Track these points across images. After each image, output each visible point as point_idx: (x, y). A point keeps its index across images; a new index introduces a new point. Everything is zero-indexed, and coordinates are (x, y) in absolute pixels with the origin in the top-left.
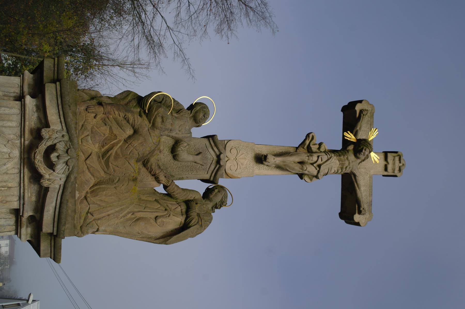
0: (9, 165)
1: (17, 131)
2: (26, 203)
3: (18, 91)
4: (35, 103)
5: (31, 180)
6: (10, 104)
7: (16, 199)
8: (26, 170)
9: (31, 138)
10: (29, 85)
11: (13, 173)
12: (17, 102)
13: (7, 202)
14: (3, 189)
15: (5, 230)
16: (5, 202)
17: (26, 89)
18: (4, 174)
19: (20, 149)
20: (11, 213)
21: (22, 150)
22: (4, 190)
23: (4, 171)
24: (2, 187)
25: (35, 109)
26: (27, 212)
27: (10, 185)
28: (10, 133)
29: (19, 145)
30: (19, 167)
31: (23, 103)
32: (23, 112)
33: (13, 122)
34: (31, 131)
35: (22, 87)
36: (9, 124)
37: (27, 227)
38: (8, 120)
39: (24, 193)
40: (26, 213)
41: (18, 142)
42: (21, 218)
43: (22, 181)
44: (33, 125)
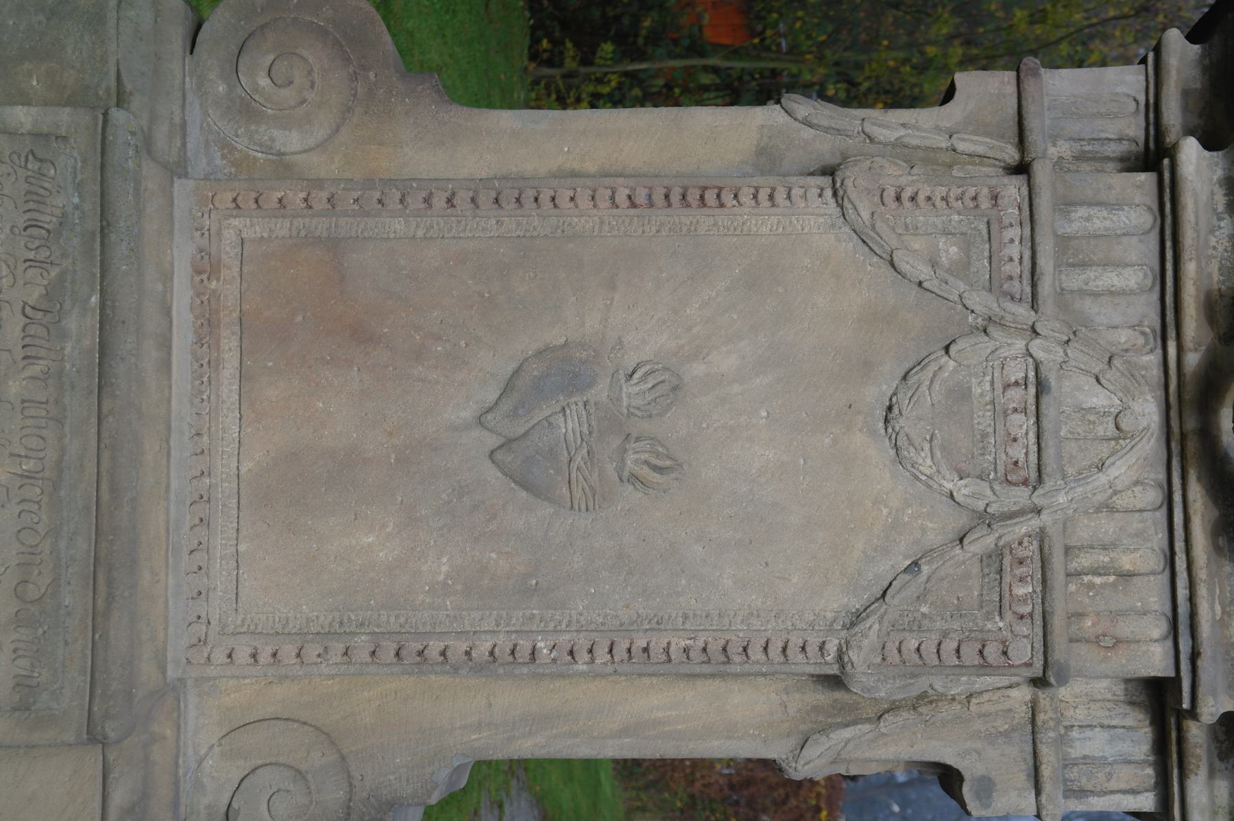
0: (1121, 470)
1: (1146, 309)
2: (1206, 650)
3: (1135, 128)
4: (1219, 173)
5: (1222, 541)
6: (1110, 187)
7: (1159, 628)
8: (1196, 492)
9: (1208, 337)
10: (1186, 93)
11: (1139, 506)
12: (1142, 177)
13: (1118, 641)
14: (1098, 580)
15: (1113, 785)
16: (1108, 642)
17: (1173, 115)
18: (1098, 510)
19: (1160, 393)
20: (1131, 703)
21: (1173, 399)
22: (1103, 586)
23: (1100, 498)
24: (1096, 572)
25: (1221, 200)
26: (1214, 694)
27: (1126, 562)
28: (1117, 319)
29: (1156, 373)
30: (1162, 476)
31: (1167, 175)
32: (1169, 220)
33: (1128, 272)
34: (1210, 306)
35: (1154, 109)
36: (1111, 279)
37: (1212, 774)
38: (1106, 264)
39: (1192, 599)
40: (1211, 701)
41: (1152, 360)
42: (1180, 729)
43: (1179, 545)
44: (1216, 277)
